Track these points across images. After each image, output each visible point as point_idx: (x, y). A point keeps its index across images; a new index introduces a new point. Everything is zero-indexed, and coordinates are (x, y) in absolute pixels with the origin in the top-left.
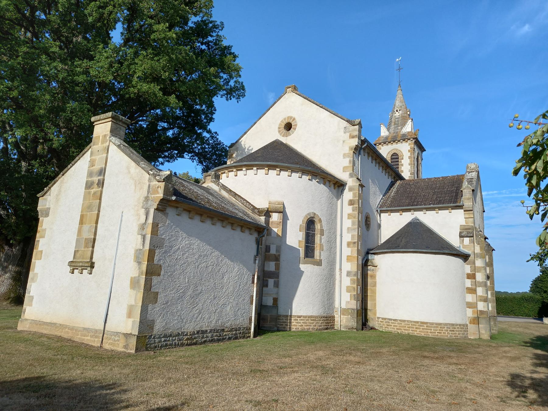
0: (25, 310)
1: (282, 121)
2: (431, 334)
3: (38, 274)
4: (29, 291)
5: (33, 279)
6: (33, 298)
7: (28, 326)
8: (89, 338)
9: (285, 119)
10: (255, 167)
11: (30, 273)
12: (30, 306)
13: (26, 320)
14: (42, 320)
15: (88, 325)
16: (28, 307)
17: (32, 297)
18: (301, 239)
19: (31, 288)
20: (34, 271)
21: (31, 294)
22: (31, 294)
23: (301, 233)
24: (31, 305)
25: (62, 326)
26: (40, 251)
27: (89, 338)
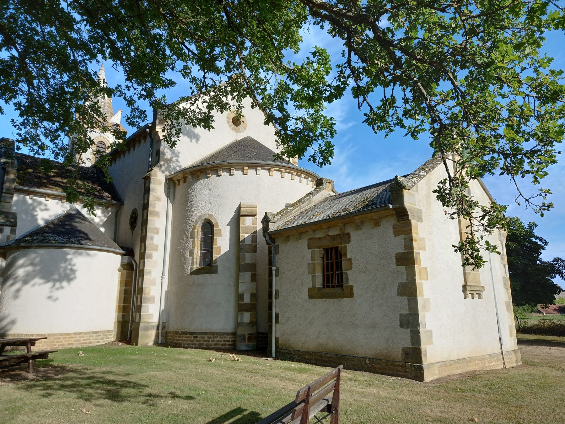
0: (426, 351)
1: (230, 126)
2: (61, 340)
3: (429, 299)
4: (424, 324)
5: (424, 307)
6: (432, 334)
7: (437, 372)
8: (494, 363)
9: (228, 122)
10: (312, 178)
11: (419, 298)
12: (429, 344)
13: (433, 364)
14: (450, 359)
15: (490, 351)
16: (428, 346)
17: (431, 331)
18: (421, 252)
19: (425, 319)
20: (422, 295)
21: (428, 328)
22: (428, 328)
23: (218, 245)
24: (431, 343)
25: (472, 360)
26: (424, 268)
27: (494, 363)
